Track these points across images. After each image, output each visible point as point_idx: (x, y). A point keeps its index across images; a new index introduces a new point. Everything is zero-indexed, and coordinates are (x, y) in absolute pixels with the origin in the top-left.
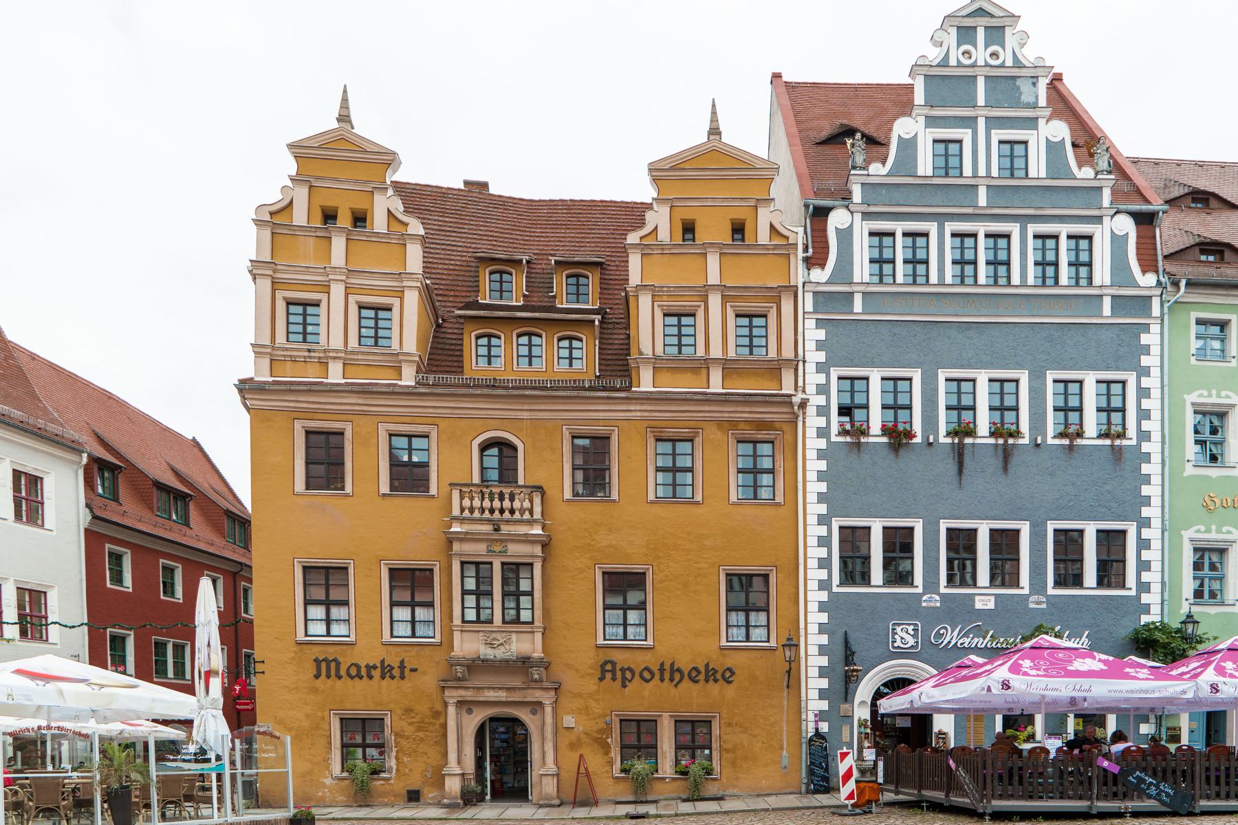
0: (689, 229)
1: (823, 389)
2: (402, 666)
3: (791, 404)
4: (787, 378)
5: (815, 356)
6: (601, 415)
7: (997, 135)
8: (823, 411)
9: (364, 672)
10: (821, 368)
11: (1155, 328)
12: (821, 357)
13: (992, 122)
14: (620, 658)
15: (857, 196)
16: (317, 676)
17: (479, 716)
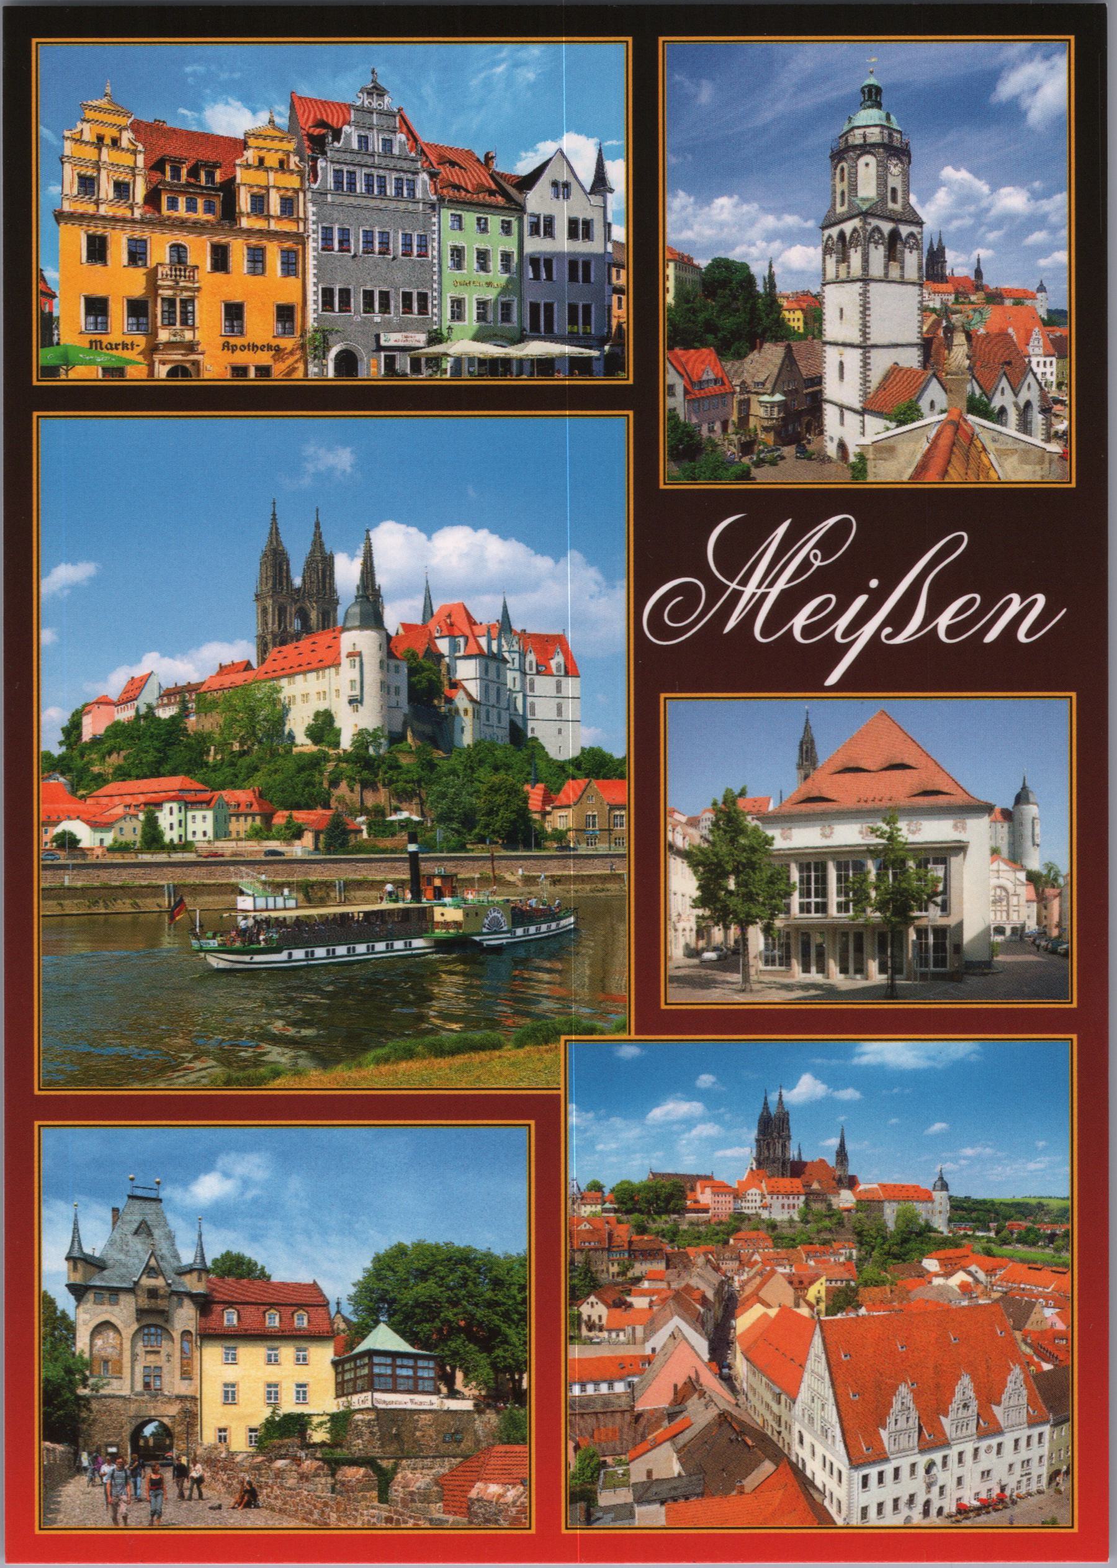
0: (261, 161)
4: (301, 225)
5: (312, 218)
8: (315, 240)
12: (314, 218)
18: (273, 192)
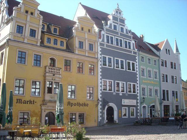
0: (82, 29)
1: (101, 58)
2: (34, 101)
3: (98, 60)
6: (70, 57)
7: (121, 26)
8: (101, 61)
9: (26, 102)
10: (101, 55)
11: (137, 57)
13: (120, 25)
14: (71, 102)
15: (105, 30)
16: (17, 103)
17: (47, 111)
18: (87, 41)
